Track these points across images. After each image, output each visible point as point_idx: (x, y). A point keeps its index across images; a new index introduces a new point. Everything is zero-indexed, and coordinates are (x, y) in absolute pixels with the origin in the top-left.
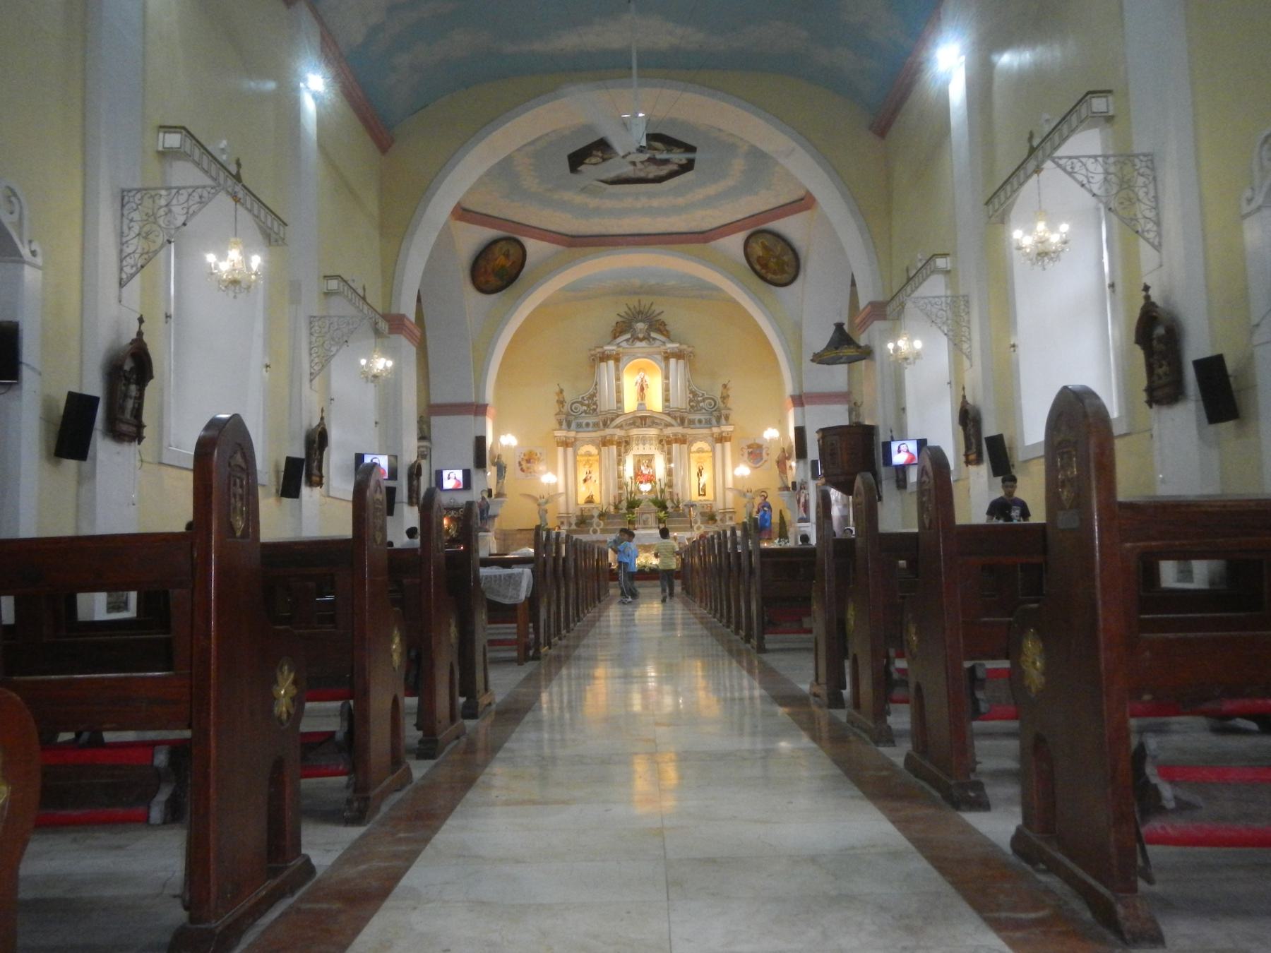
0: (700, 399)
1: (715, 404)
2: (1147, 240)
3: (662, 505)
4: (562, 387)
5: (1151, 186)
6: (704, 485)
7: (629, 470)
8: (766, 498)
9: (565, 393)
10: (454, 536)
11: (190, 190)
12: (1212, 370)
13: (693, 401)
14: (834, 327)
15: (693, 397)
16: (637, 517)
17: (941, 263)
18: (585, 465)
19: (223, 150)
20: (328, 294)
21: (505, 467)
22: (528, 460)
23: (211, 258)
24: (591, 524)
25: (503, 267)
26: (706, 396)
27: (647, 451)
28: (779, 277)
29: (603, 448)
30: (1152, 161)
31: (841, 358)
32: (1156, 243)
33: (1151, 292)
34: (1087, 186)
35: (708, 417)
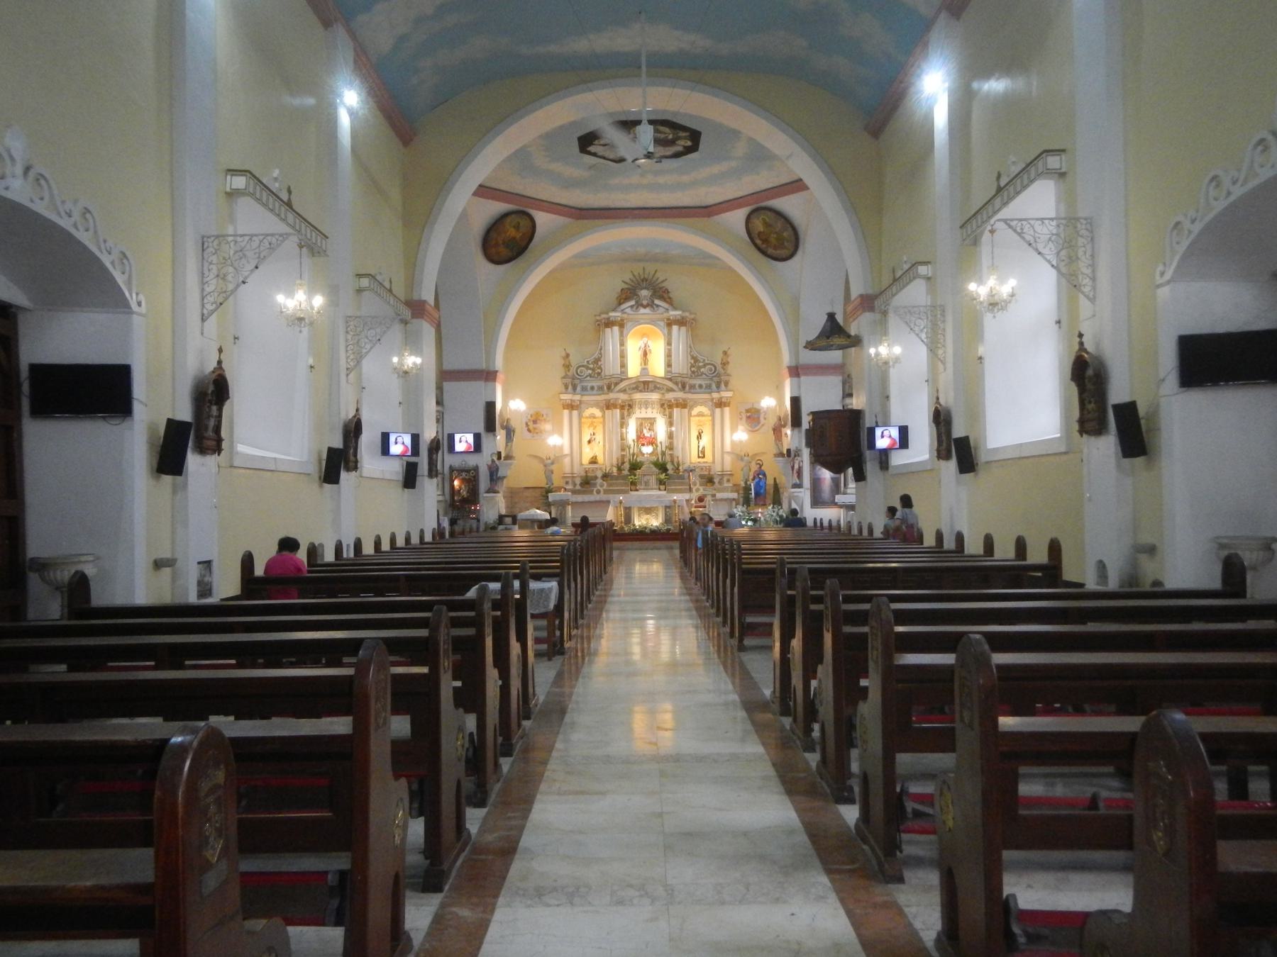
0: (701, 364)
1: (715, 372)
2: (1083, 293)
3: (662, 468)
4: (568, 351)
5: (1089, 247)
6: (704, 448)
7: (631, 434)
8: (761, 466)
9: (571, 357)
10: (465, 496)
11: (261, 237)
12: (1127, 413)
14: (826, 316)
15: (695, 362)
17: (922, 270)
19: (276, 179)
20: (360, 291)
21: (514, 431)
22: (534, 421)
23: (280, 298)
24: (595, 485)
25: (514, 238)
26: (706, 362)
27: (649, 415)
28: (778, 252)
29: (607, 412)
30: (1091, 224)
31: (832, 346)
32: (1091, 295)
33: (1084, 339)
34: (1034, 245)
35: (708, 382)
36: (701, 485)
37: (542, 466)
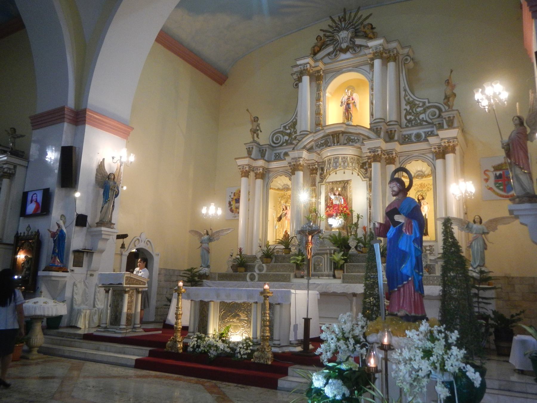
0: (419, 110)
9: (259, 122)
13: (410, 114)
15: (411, 108)
26: (427, 105)
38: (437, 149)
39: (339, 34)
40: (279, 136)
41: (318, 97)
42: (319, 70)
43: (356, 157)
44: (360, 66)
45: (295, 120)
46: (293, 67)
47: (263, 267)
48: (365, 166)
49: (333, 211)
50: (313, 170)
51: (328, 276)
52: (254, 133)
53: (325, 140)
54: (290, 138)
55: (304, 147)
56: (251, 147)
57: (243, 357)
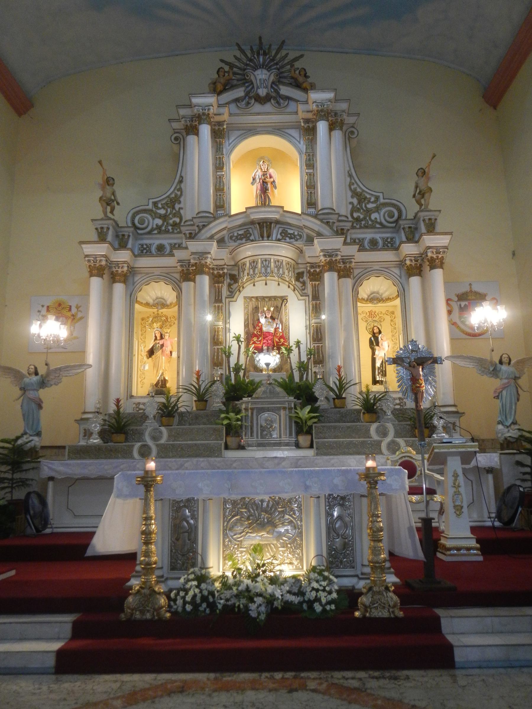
0: (370, 206)
9: (115, 187)
13: (358, 210)
15: (360, 202)
16: (246, 416)
18: (153, 322)
26: (382, 200)
29: (184, 285)
36: (398, 434)
37: (17, 389)
38: (414, 261)
39: (256, 73)
40: (146, 218)
41: (220, 164)
42: (220, 122)
43: (293, 262)
44: (285, 129)
45: (173, 196)
46: (178, 107)
47: (161, 432)
48: (302, 278)
49: (264, 343)
50: (220, 276)
51: (287, 444)
52: (108, 204)
53: (245, 230)
54: (165, 223)
55: (211, 238)
56: (107, 226)
57: (328, 607)
